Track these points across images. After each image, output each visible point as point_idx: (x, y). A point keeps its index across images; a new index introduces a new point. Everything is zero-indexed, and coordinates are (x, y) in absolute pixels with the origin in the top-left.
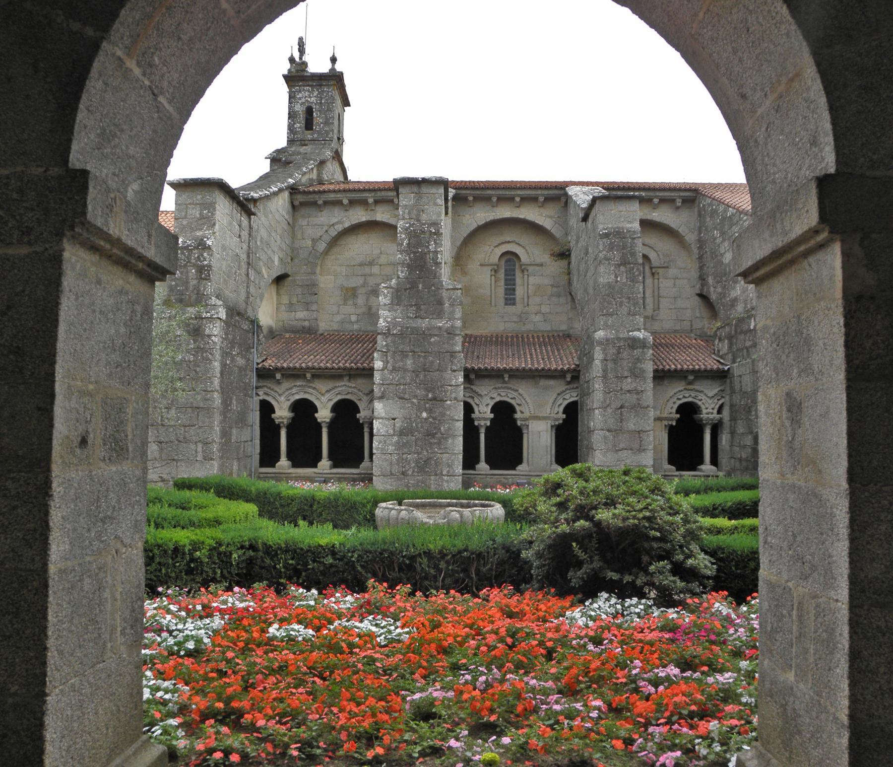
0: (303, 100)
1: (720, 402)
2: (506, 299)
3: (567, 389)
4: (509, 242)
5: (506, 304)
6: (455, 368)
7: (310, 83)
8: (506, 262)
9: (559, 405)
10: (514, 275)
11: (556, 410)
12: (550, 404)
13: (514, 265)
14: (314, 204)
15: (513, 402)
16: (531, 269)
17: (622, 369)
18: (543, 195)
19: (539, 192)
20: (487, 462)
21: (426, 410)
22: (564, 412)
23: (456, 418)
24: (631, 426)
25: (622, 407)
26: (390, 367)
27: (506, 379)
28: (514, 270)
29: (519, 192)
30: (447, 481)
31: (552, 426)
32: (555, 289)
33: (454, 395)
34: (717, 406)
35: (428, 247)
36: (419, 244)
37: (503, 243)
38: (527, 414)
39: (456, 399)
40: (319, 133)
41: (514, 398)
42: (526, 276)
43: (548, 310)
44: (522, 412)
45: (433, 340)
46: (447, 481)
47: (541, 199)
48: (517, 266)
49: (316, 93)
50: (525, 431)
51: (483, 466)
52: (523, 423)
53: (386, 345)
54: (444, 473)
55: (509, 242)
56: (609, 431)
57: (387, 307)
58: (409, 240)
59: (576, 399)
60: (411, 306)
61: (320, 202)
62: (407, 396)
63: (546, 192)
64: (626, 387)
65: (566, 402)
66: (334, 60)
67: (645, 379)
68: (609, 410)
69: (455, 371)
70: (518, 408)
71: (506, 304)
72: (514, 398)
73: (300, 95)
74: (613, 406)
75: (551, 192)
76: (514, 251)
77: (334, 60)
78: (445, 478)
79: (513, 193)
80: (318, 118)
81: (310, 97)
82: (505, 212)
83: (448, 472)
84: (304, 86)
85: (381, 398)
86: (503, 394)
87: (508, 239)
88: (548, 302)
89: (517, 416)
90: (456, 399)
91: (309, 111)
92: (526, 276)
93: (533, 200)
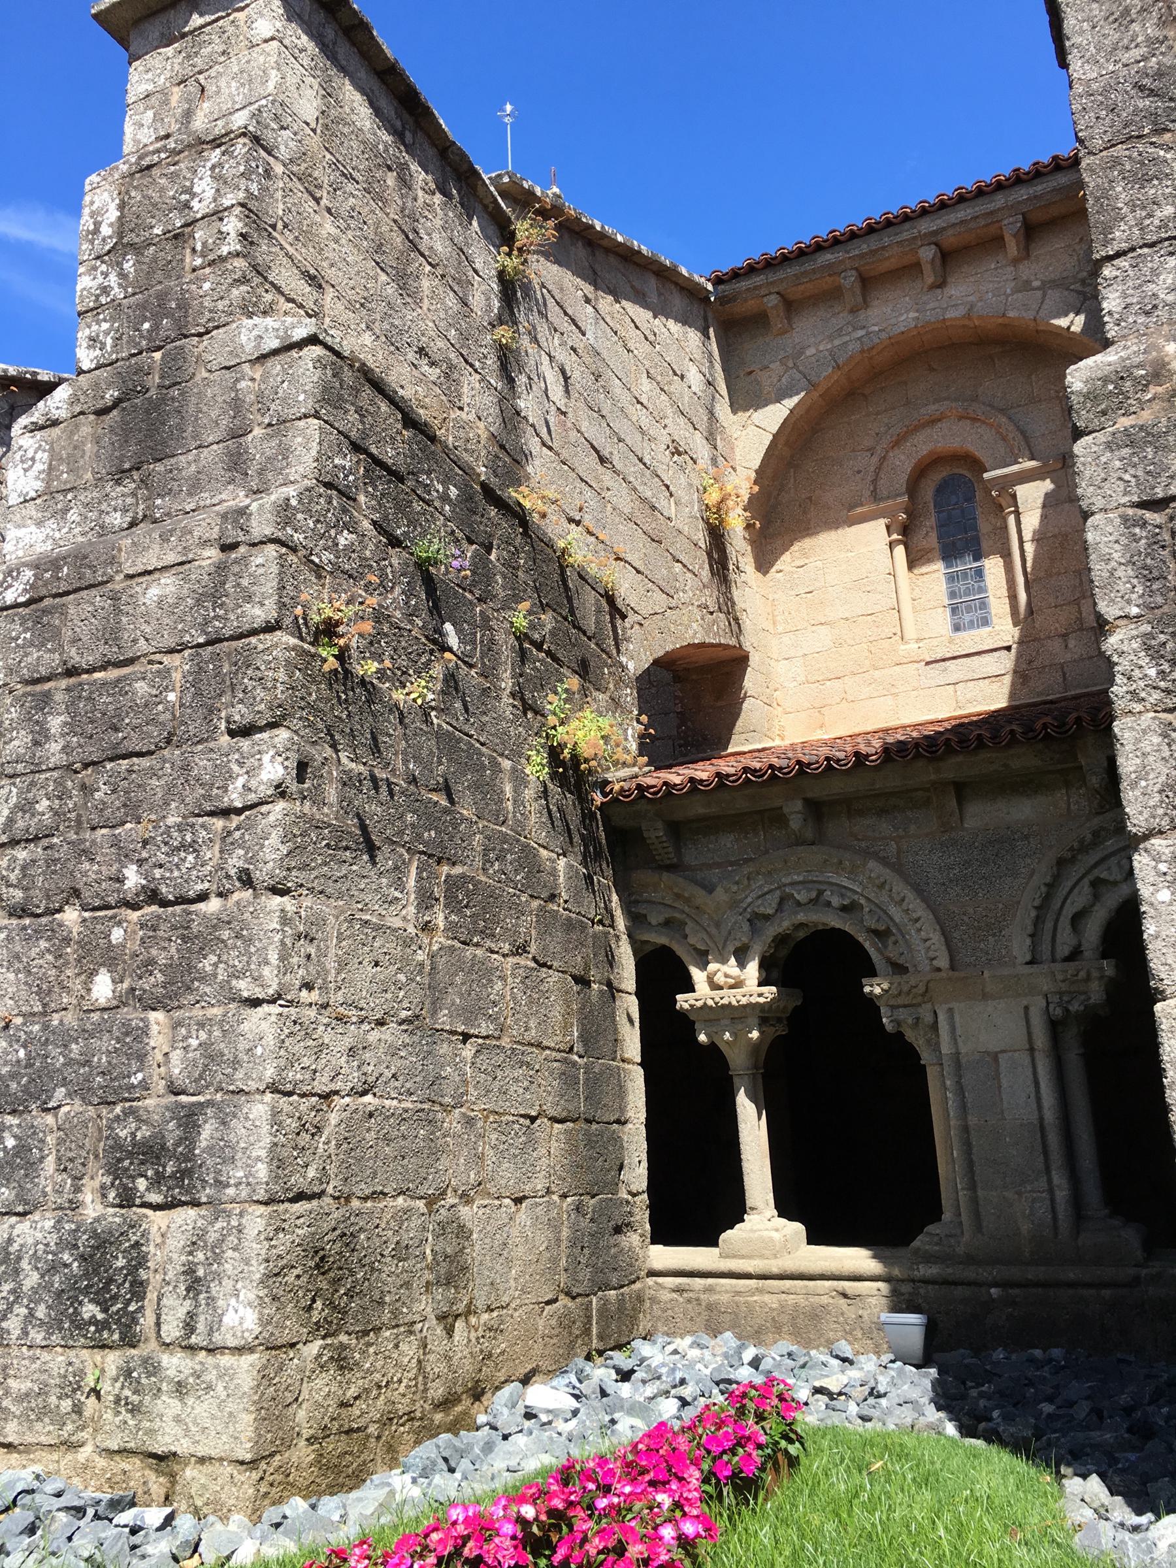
2: (954, 610)
5: (957, 628)
6: (240, 714)
8: (940, 490)
9: (1077, 919)
10: (975, 529)
11: (1066, 941)
12: (1025, 916)
13: (970, 498)
19: (999, 200)
20: (785, 1209)
23: (245, 987)
29: (926, 226)
33: (235, 862)
37: (917, 429)
45: (154, 592)
47: (1011, 226)
51: (766, 1232)
57: (31, 510)
63: (1022, 193)
69: (246, 731)
71: (957, 628)
75: (1039, 188)
79: (907, 232)
82: (897, 314)
90: (246, 880)
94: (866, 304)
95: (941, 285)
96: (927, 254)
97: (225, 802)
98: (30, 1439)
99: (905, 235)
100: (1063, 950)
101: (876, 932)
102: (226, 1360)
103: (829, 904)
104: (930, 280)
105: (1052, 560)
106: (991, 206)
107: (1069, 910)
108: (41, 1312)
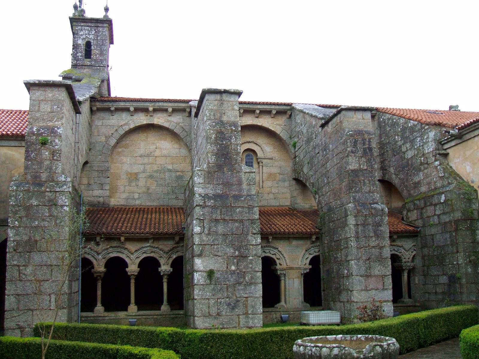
0: (84, 37)
1: (413, 254)
3: (312, 247)
4: (249, 142)
7: (89, 24)
8: (247, 156)
11: (305, 262)
12: (300, 259)
13: (252, 159)
14: (108, 110)
15: (274, 257)
16: (264, 161)
17: (369, 230)
18: (275, 109)
19: (273, 107)
21: (234, 264)
22: (310, 264)
23: (257, 269)
24: (377, 272)
25: (369, 259)
26: (206, 231)
27: (270, 240)
28: (252, 162)
29: (259, 107)
30: (252, 318)
31: (302, 274)
32: (281, 176)
33: (254, 252)
34: (412, 257)
35: (230, 141)
36: (224, 138)
37: (245, 143)
38: (284, 266)
39: (256, 255)
40: (96, 61)
41: (275, 254)
42: (261, 167)
43: (277, 191)
44: (280, 264)
45: (238, 210)
46: (252, 318)
48: (254, 159)
49: (93, 32)
50: (283, 278)
52: (282, 272)
53: (203, 214)
54: (250, 312)
55: (249, 142)
56: (361, 276)
58: (216, 135)
59: (317, 254)
60: (219, 184)
61: (113, 109)
62: (219, 254)
63: (277, 107)
64: (373, 244)
65: (311, 256)
66: (107, 10)
67: (384, 239)
68: (361, 262)
70: (278, 261)
72: (275, 254)
73: (82, 33)
74: (364, 258)
76: (253, 149)
77: (107, 10)
78: (250, 316)
80: (95, 51)
81: (89, 35)
83: (252, 311)
84: (85, 26)
85: (200, 256)
86: (267, 251)
87: (249, 140)
88: (277, 185)
89: (278, 267)
91: (88, 45)
92: (261, 167)
93: (269, 112)
94: (242, 116)
95: (257, 117)
96: (258, 112)
97: (252, 244)
98: (228, 327)
99: (255, 107)
100: (304, 264)
101: (278, 259)
102: (258, 315)
103: (270, 253)
104: (257, 116)
105: (268, 178)
106: (272, 108)
107: (305, 258)
108: (228, 311)
